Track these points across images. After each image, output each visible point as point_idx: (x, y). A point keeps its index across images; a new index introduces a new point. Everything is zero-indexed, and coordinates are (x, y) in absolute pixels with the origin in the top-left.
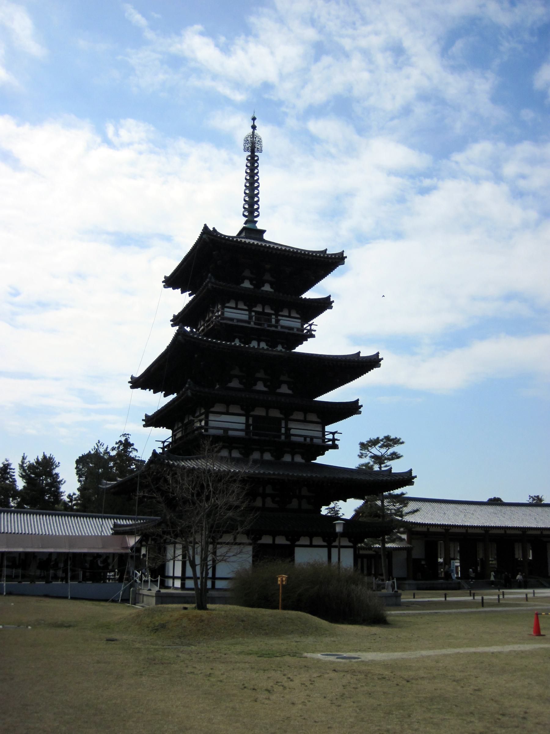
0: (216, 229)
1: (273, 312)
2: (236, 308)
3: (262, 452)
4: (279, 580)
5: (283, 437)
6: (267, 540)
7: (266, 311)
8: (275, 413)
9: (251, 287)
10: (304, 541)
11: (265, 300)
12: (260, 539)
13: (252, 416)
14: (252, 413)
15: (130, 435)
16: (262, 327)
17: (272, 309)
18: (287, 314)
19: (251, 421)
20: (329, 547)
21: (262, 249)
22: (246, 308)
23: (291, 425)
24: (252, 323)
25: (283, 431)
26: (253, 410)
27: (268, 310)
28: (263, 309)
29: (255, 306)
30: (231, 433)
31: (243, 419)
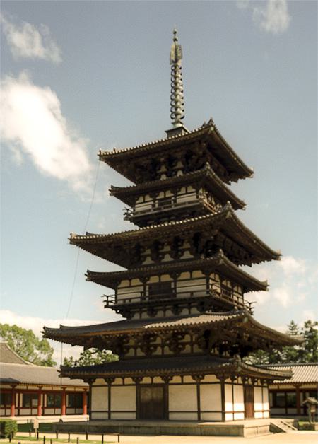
0: (110, 151)
1: (172, 195)
3: (165, 310)
4: (56, 410)
6: (147, 380)
7: (167, 196)
10: (177, 379)
11: (164, 188)
12: (142, 380)
13: (148, 284)
14: (148, 282)
15: (255, 302)
19: (147, 287)
20: (198, 384)
21: (141, 149)
22: (151, 199)
24: (173, 207)
26: (148, 280)
29: (158, 195)
30: (133, 301)
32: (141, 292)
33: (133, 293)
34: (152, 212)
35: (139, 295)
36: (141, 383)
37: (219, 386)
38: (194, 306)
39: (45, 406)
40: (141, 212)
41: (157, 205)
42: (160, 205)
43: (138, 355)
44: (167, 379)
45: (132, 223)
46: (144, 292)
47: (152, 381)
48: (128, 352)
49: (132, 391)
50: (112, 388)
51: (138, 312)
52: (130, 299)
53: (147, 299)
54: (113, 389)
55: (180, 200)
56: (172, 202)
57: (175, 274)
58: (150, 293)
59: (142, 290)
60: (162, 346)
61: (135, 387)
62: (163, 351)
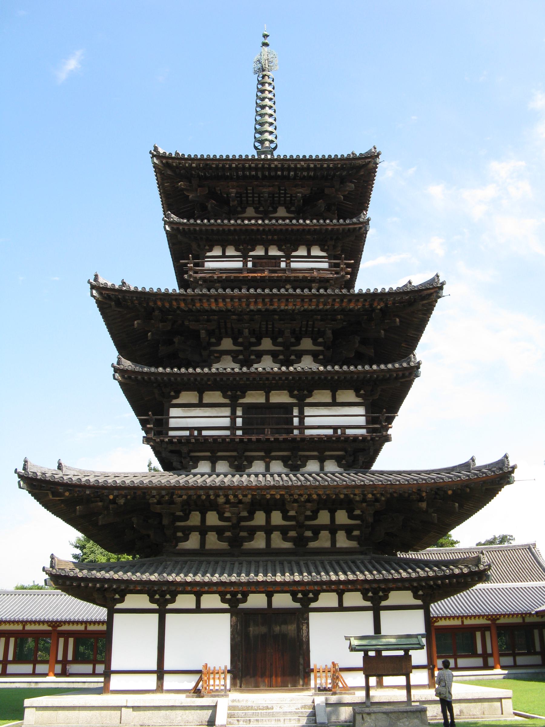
5: (296, 432)
12: (244, 600)
13: (241, 405)
14: (241, 401)
16: (263, 275)
17: (280, 250)
18: (305, 254)
19: (239, 413)
23: (308, 411)
25: (296, 421)
26: (243, 397)
27: (274, 252)
28: (266, 251)
29: (253, 250)
31: (227, 412)
35: (226, 422)
36: (242, 606)
37: (370, 615)
38: (331, 458)
39: (70, 657)
42: (254, 265)
43: (208, 547)
47: (270, 602)
48: (186, 538)
50: (169, 617)
51: (204, 458)
52: (200, 429)
53: (239, 433)
54: (169, 617)
55: (294, 265)
60: (268, 529)
61: (228, 616)
62: (268, 541)
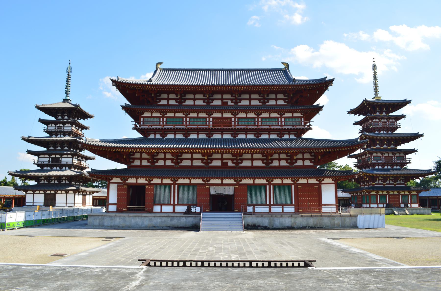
2: (52, 126)
8: (58, 156)
9: (61, 118)
12: (46, 192)
14: (51, 157)
22: (54, 125)
23: (63, 159)
31: (48, 159)
32: (48, 160)
33: (45, 159)
34: (54, 131)
35: (48, 161)
40: (50, 130)
41: (56, 129)
44: (56, 192)
45: (46, 133)
46: (49, 160)
49: (43, 196)
50: (35, 194)
53: (50, 163)
54: (35, 194)
56: (63, 129)
57: (62, 155)
58: (52, 161)
59: (49, 159)
61: (44, 194)
